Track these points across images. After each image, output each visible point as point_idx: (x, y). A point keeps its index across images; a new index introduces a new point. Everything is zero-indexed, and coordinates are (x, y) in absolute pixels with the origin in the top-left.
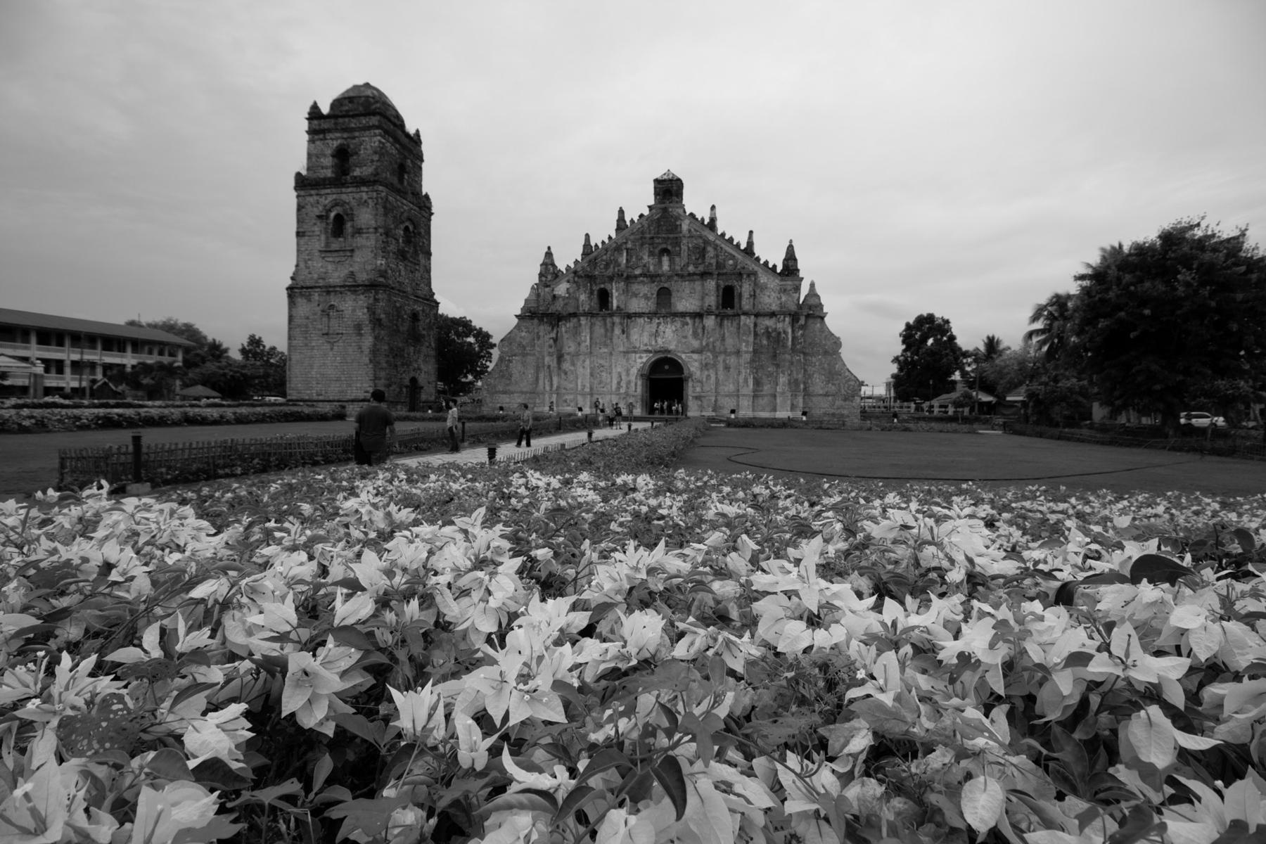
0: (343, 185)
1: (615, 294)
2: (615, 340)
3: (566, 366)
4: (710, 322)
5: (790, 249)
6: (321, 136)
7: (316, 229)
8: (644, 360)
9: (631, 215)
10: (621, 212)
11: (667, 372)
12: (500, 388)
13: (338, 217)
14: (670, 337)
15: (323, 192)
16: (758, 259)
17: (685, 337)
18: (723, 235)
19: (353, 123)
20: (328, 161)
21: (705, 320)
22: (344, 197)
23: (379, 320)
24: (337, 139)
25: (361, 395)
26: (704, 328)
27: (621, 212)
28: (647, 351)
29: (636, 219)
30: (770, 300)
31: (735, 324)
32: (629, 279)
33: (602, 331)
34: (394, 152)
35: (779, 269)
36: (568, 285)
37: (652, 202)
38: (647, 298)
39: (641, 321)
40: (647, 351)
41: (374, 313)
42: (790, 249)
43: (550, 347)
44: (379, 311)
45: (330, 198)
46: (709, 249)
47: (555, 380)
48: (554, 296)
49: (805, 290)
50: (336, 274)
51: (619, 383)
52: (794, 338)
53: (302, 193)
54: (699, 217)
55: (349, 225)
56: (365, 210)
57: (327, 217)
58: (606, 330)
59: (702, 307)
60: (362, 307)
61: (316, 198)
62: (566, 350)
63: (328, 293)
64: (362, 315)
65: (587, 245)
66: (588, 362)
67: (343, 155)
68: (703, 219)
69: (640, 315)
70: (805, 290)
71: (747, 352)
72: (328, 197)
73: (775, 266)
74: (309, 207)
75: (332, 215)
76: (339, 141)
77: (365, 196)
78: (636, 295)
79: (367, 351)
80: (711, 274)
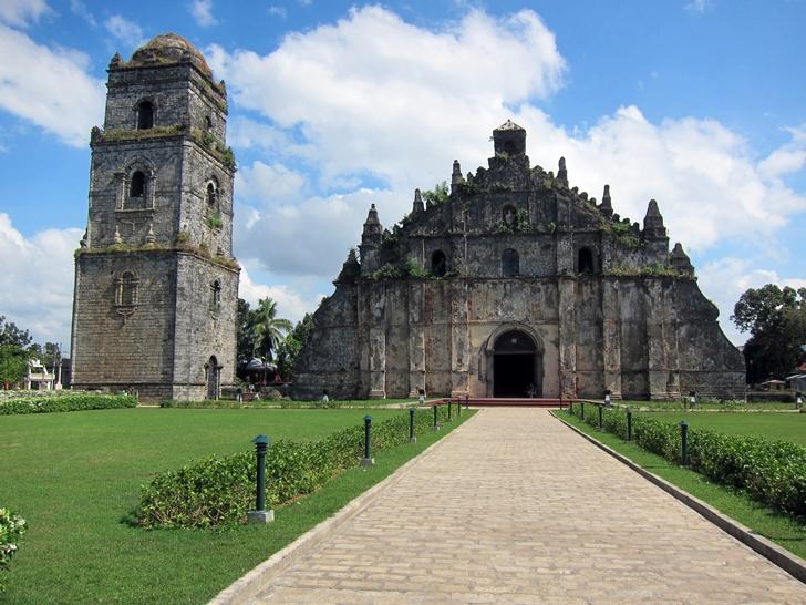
4: (568, 289)
5: (653, 205)
6: (122, 89)
10: (456, 165)
11: (515, 346)
12: (314, 367)
14: (519, 308)
16: (617, 217)
17: (538, 306)
18: (576, 189)
21: (560, 286)
23: (182, 289)
24: (143, 90)
27: (456, 165)
28: (492, 323)
30: (633, 265)
34: (201, 104)
35: (641, 228)
37: (492, 155)
39: (483, 287)
40: (492, 323)
41: (176, 281)
42: (653, 205)
49: (671, 247)
53: (99, 149)
54: (547, 170)
61: (114, 154)
62: (395, 322)
65: (418, 204)
68: (551, 173)
70: (671, 247)
73: (637, 225)
75: (131, 173)
76: (142, 95)
78: (476, 258)
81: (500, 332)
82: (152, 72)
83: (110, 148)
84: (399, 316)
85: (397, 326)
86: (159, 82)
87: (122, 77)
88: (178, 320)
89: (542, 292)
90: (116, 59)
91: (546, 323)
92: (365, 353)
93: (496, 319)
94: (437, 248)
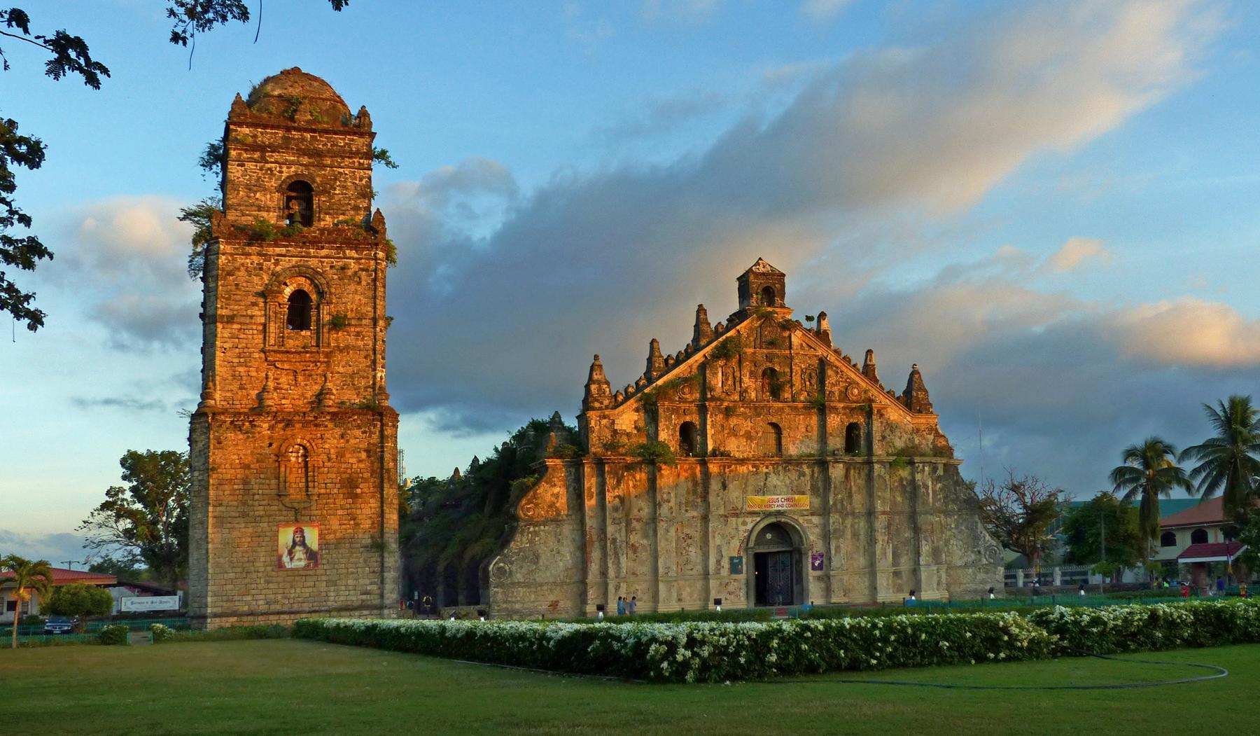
0: (316, 243)
1: (710, 431)
2: (712, 499)
3: (635, 538)
6: (257, 155)
7: (256, 311)
8: (749, 527)
9: (718, 317)
10: (701, 310)
13: (299, 296)
15: (271, 250)
19: (322, 143)
20: (275, 199)
21: (831, 470)
22: (313, 263)
23: (388, 471)
24: (289, 164)
25: (356, 599)
26: (827, 480)
27: (701, 310)
29: (725, 323)
31: (863, 474)
32: (728, 412)
33: (690, 484)
36: (635, 416)
38: (748, 436)
41: (382, 458)
43: (616, 509)
44: (387, 456)
45: (285, 263)
46: (830, 372)
47: (623, 559)
48: (615, 431)
50: (294, 392)
51: (718, 562)
52: (934, 492)
53: (229, 249)
55: (325, 310)
56: (352, 287)
57: (281, 292)
58: (695, 484)
59: (823, 451)
60: (356, 450)
61: (256, 259)
63: (289, 424)
64: (357, 463)
66: (673, 530)
67: (300, 190)
69: (742, 461)
71: (884, 513)
72: (284, 258)
74: (242, 273)
75: (288, 291)
77: (353, 266)
78: (734, 433)
79: (366, 524)
80: (836, 408)
81: (762, 525)
82: (308, 136)
83: (248, 249)
84: (642, 508)
85: (638, 520)
86: (318, 154)
87: (255, 136)
88: (387, 516)
89: (808, 478)
90: (237, 102)
91: (812, 514)
92: (595, 555)
93: (757, 509)
94: (688, 419)
